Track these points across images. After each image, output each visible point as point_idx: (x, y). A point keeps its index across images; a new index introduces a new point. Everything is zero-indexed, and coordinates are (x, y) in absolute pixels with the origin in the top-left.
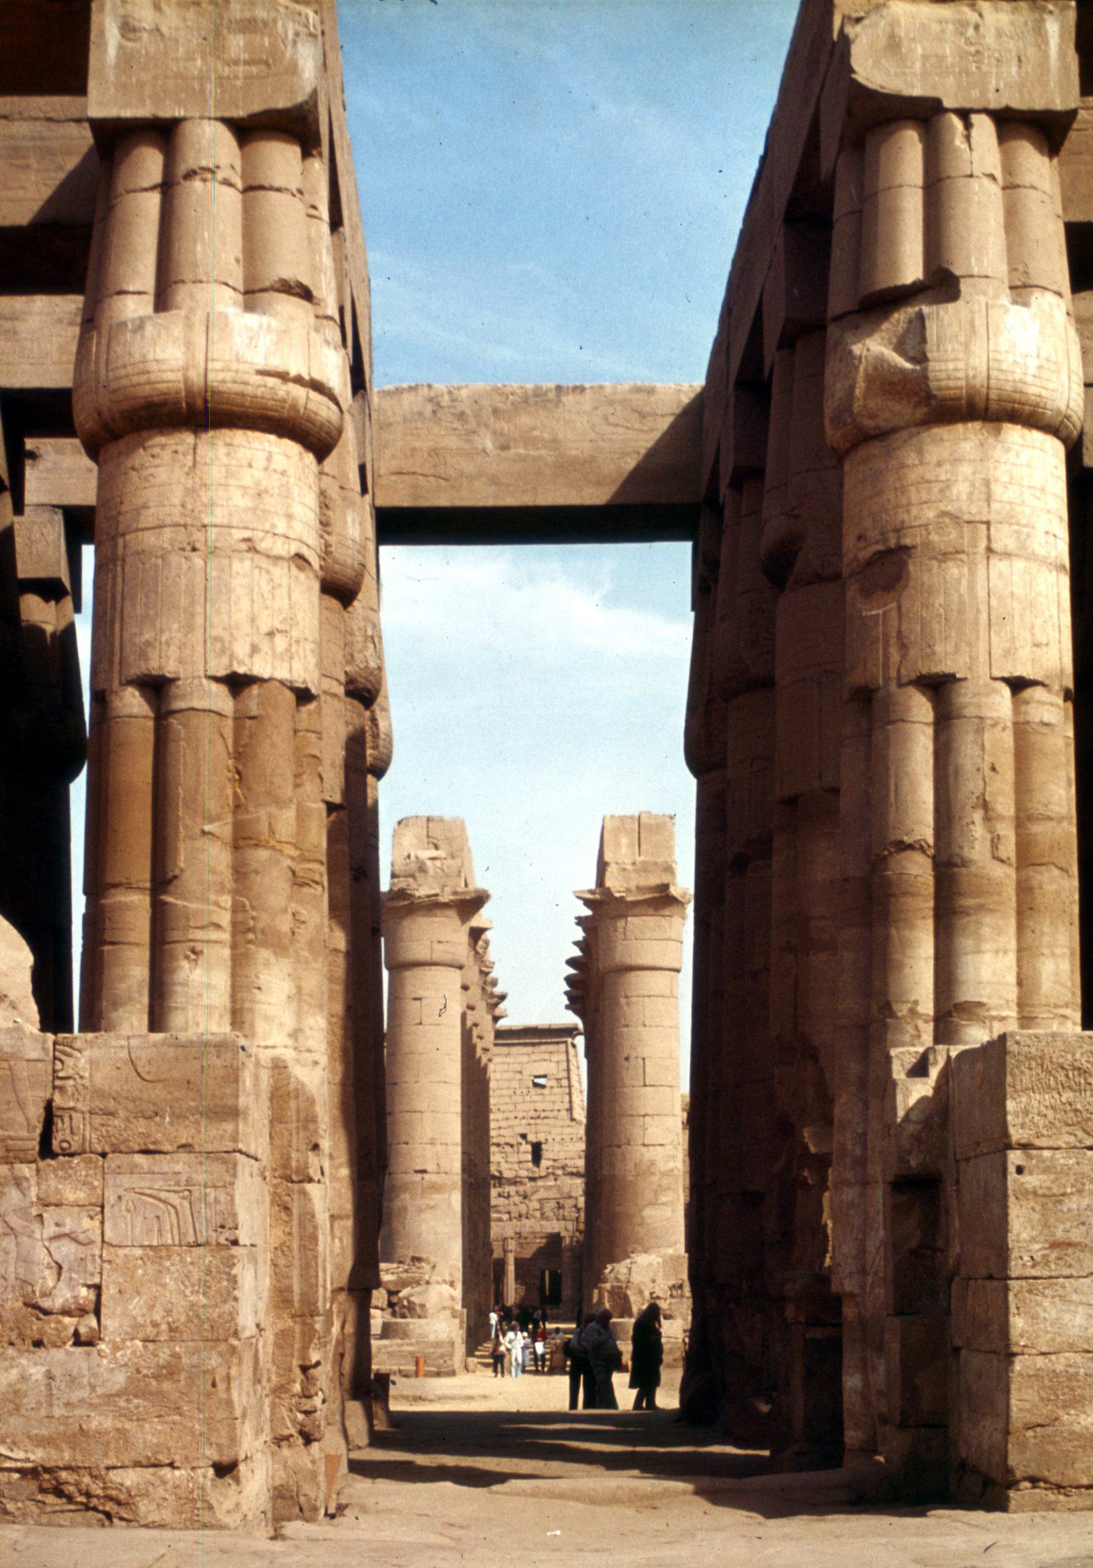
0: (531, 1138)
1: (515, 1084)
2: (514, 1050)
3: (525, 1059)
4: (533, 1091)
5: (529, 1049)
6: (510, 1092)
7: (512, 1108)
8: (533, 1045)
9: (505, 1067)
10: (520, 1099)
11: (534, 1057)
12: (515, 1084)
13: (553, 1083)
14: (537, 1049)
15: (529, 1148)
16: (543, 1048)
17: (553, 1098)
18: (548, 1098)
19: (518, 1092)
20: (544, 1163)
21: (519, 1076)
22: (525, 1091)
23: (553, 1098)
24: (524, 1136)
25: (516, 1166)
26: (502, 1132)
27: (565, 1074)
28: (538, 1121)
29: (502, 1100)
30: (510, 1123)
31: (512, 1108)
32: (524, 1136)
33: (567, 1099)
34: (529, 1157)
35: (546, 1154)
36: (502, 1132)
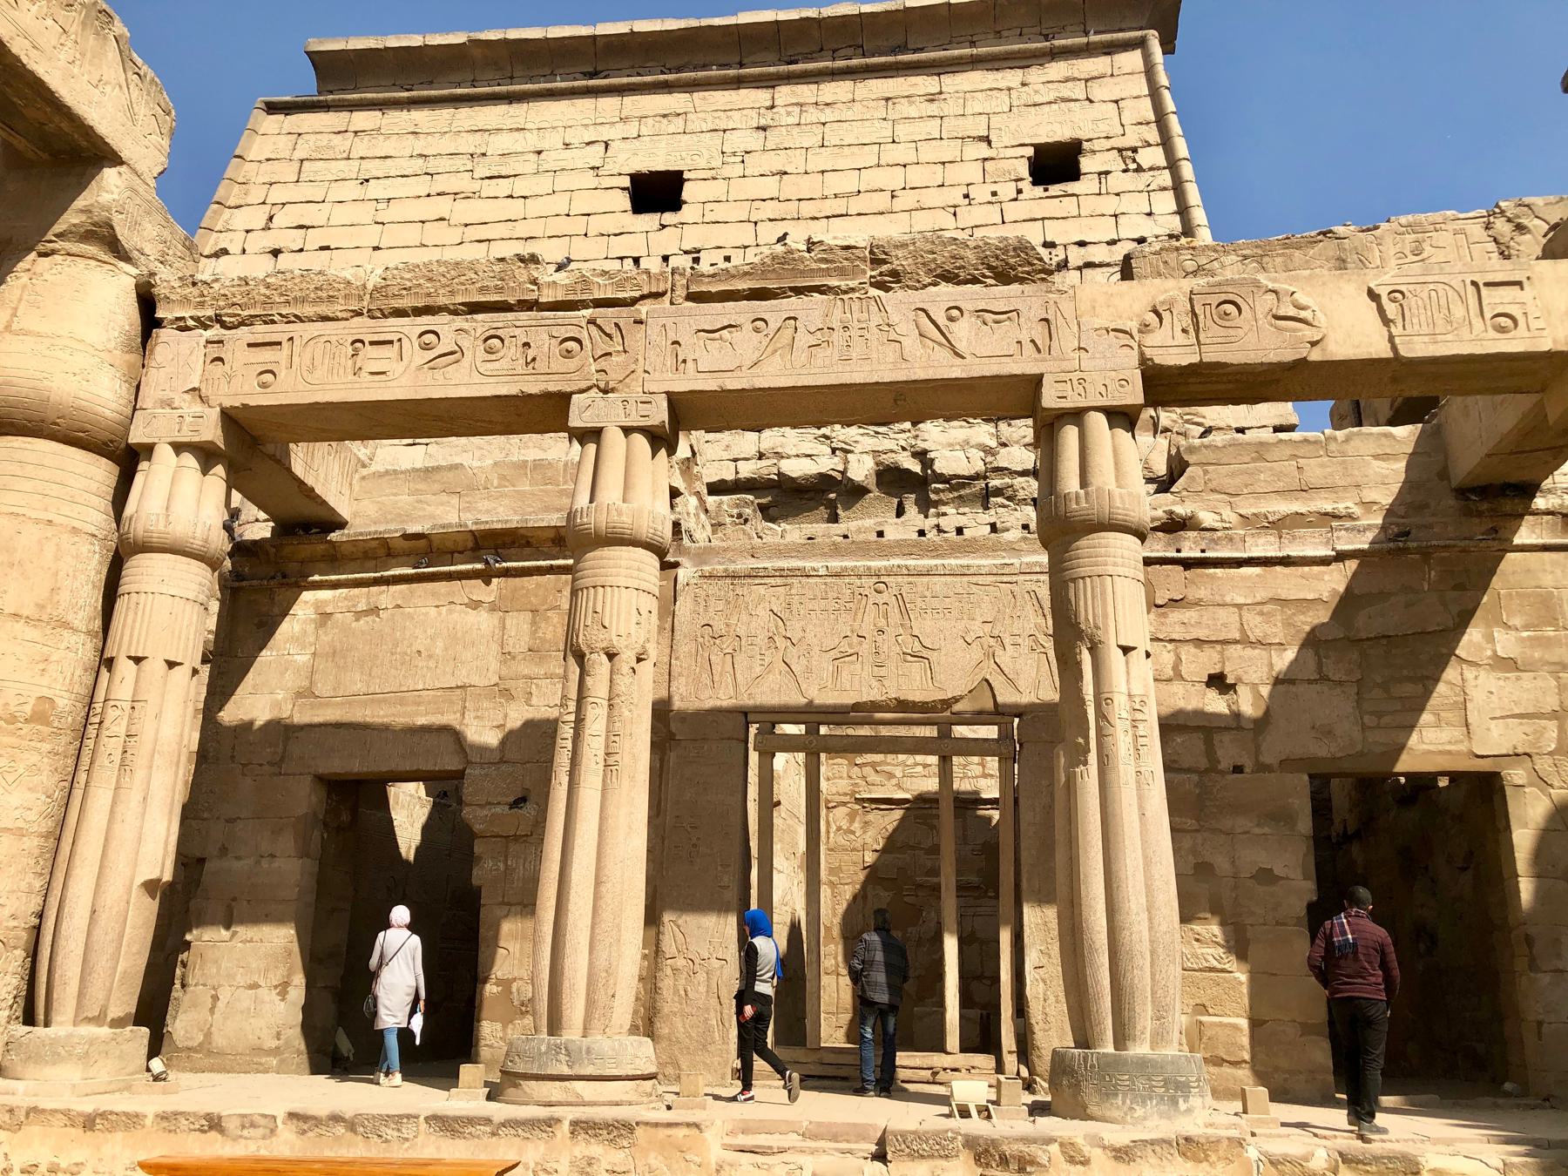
1: (972, 172)
3: (1001, 102)
5: (1012, 77)
6: (956, 196)
9: (932, 128)
11: (1026, 95)
13: (1113, 162)
14: (1035, 75)
16: (1058, 69)
17: (1109, 205)
18: (1088, 205)
19: (981, 193)
21: (983, 150)
22: (1007, 191)
23: (1109, 205)
27: (1153, 134)
33: (1166, 202)
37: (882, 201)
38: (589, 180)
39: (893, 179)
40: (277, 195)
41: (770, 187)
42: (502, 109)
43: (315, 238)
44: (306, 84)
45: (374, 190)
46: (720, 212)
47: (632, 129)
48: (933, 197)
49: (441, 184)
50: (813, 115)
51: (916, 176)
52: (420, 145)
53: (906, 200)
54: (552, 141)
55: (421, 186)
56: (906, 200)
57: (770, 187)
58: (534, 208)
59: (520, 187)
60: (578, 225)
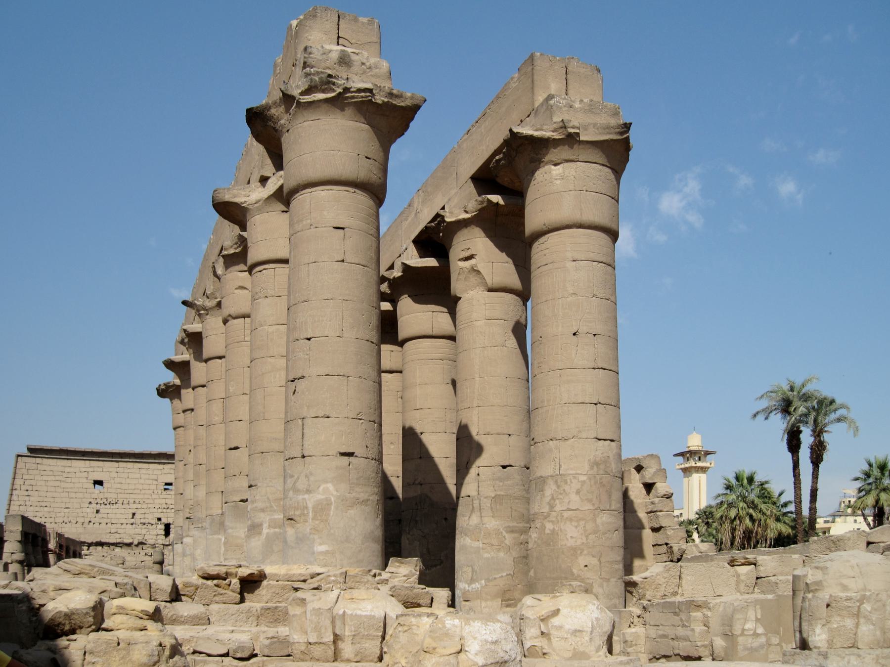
0: (164, 521)
1: (153, 487)
2: (151, 466)
4: (164, 493)
5: (161, 466)
7: (152, 501)
8: (164, 463)
10: (157, 496)
12: (153, 487)
15: (163, 527)
19: (156, 492)
20: (172, 535)
21: (155, 482)
24: (159, 519)
25: (155, 537)
26: (147, 516)
28: (169, 510)
29: (146, 496)
30: (152, 510)
31: (152, 501)
32: (159, 519)
34: (163, 533)
35: (172, 530)
36: (147, 516)
37: (138, 491)
38: (85, 480)
39: (141, 487)
40: (25, 477)
41: (119, 486)
42: (66, 461)
43: (35, 488)
44: (26, 452)
45: (45, 478)
46: (110, 490)
47: (92, 470)
48: (147, 492)
49: (57, 478)
50: (126, 471)
51: (145, 487)
52: (51, 468)
53: (143, 492)
54: (77, 470)
55: (52, 478)
56: (143, 492)
57: (119, 486)
58: (77, 485)
59: (73, 480)
60: (85, 490)
